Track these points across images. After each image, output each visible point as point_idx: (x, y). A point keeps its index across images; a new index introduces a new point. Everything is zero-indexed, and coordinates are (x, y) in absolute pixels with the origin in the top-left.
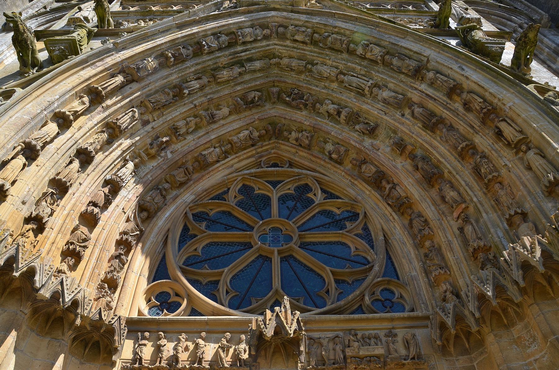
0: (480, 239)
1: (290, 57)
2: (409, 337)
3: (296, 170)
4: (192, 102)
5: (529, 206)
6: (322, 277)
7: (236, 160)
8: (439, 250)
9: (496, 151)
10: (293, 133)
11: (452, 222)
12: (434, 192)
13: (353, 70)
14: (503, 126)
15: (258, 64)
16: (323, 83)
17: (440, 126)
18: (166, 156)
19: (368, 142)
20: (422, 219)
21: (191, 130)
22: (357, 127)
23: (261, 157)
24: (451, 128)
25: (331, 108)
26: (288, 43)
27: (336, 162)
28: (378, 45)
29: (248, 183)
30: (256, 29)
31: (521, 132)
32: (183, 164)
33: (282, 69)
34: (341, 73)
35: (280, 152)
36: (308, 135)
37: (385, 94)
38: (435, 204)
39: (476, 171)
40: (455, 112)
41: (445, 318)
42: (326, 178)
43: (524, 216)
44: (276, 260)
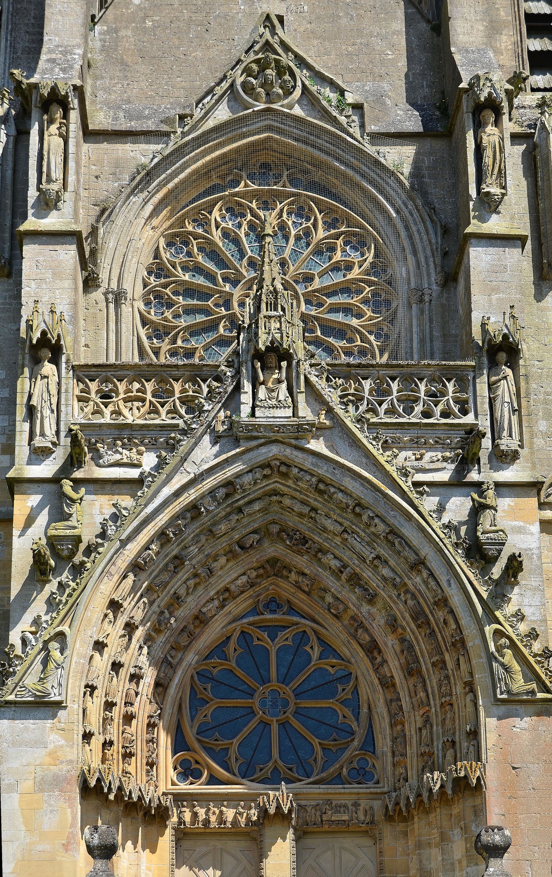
1: (294, 498)
3: (296, 619)
6: (312, 745)
10: (293, 573)
11: (418, 718)
15: (257, 506)
16: (326, 535)
19: (365, 608)
21: (191, 590)
23: (259, 595)
25: (334, 564)
26: (290, 483)
27: (335, 616)
28: (383, 521)
29: (246, 630)
32: (185, 627)
33: (282, 508)
34: (345, 531)
35: (278, 589)
36: (308, 583)
37: (385, 572)
38: (411, 697)
42: (324, 631)
43: (453, 742)
44: (275, 727)
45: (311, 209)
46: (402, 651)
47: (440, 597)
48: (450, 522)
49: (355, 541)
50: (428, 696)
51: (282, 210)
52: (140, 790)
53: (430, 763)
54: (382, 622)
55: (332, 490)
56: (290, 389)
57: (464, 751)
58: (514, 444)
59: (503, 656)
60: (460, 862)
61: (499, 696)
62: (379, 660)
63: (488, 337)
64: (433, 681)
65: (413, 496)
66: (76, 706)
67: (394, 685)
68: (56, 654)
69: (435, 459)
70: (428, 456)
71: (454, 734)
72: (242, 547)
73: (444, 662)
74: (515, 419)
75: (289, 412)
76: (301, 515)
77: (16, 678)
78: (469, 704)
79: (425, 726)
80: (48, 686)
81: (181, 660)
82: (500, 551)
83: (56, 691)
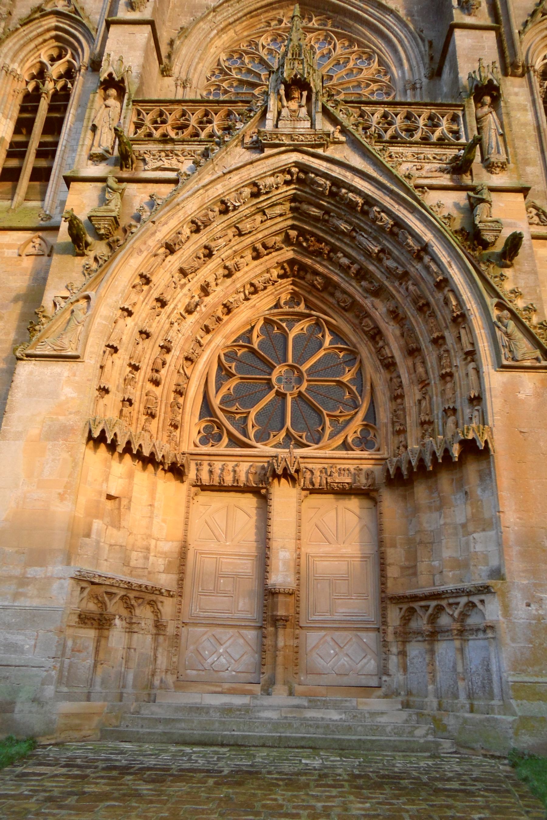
0: (427, 415)
2: (369, 473)
4: (219, 257)
5: (458, 406)
7: (258, 300)
8: (404, 410)
9: (454, 350)
11: (417, 391)
12: (410, 363)
13: (365, 231)
14: (463, 332)
17: (425, 308)
18: (201, 310)
20: (399, 380)
22: (363, 283)
24: (433, 315)
30: (277, 177)
31: (473, 344)
38: (409, 373)
39: (440, 358)
40: (437, 301)
41: (389, 467)
43: (454, 410)
45: (332, 38)
46: (402, 335)
47: (441, 278)
48: (449, 215)
49: (362, 238)
50: (426, 372)
51: (311, 39)
52: (154, 445)
53: (430, 430)
54: (384, 310)
55: (344, 191)
56: (309, 113)
57: (467, 418)
58: (503, 157)
59: (506, 327)
60: (464, 526)
61: (505, 362)
62: (381, 344)
63: (475, 83)
64: (431, 357)
65: (417, 193)
66: (93, 362)
67: (394, 364)
68: (80, 315)
69: (434, 169)
70: (427, 167)
71: (454, 402)
72: (265, 247)
73: (443, 338)
74: (501, 143)
75: (308, 124)
76: (316, 219)
77: (39, 334)
78: (472, 373)
79: (424, 398)
80: (66, 341)
81: (210, 341)
82: (496, 238)
83: (73, 346)
